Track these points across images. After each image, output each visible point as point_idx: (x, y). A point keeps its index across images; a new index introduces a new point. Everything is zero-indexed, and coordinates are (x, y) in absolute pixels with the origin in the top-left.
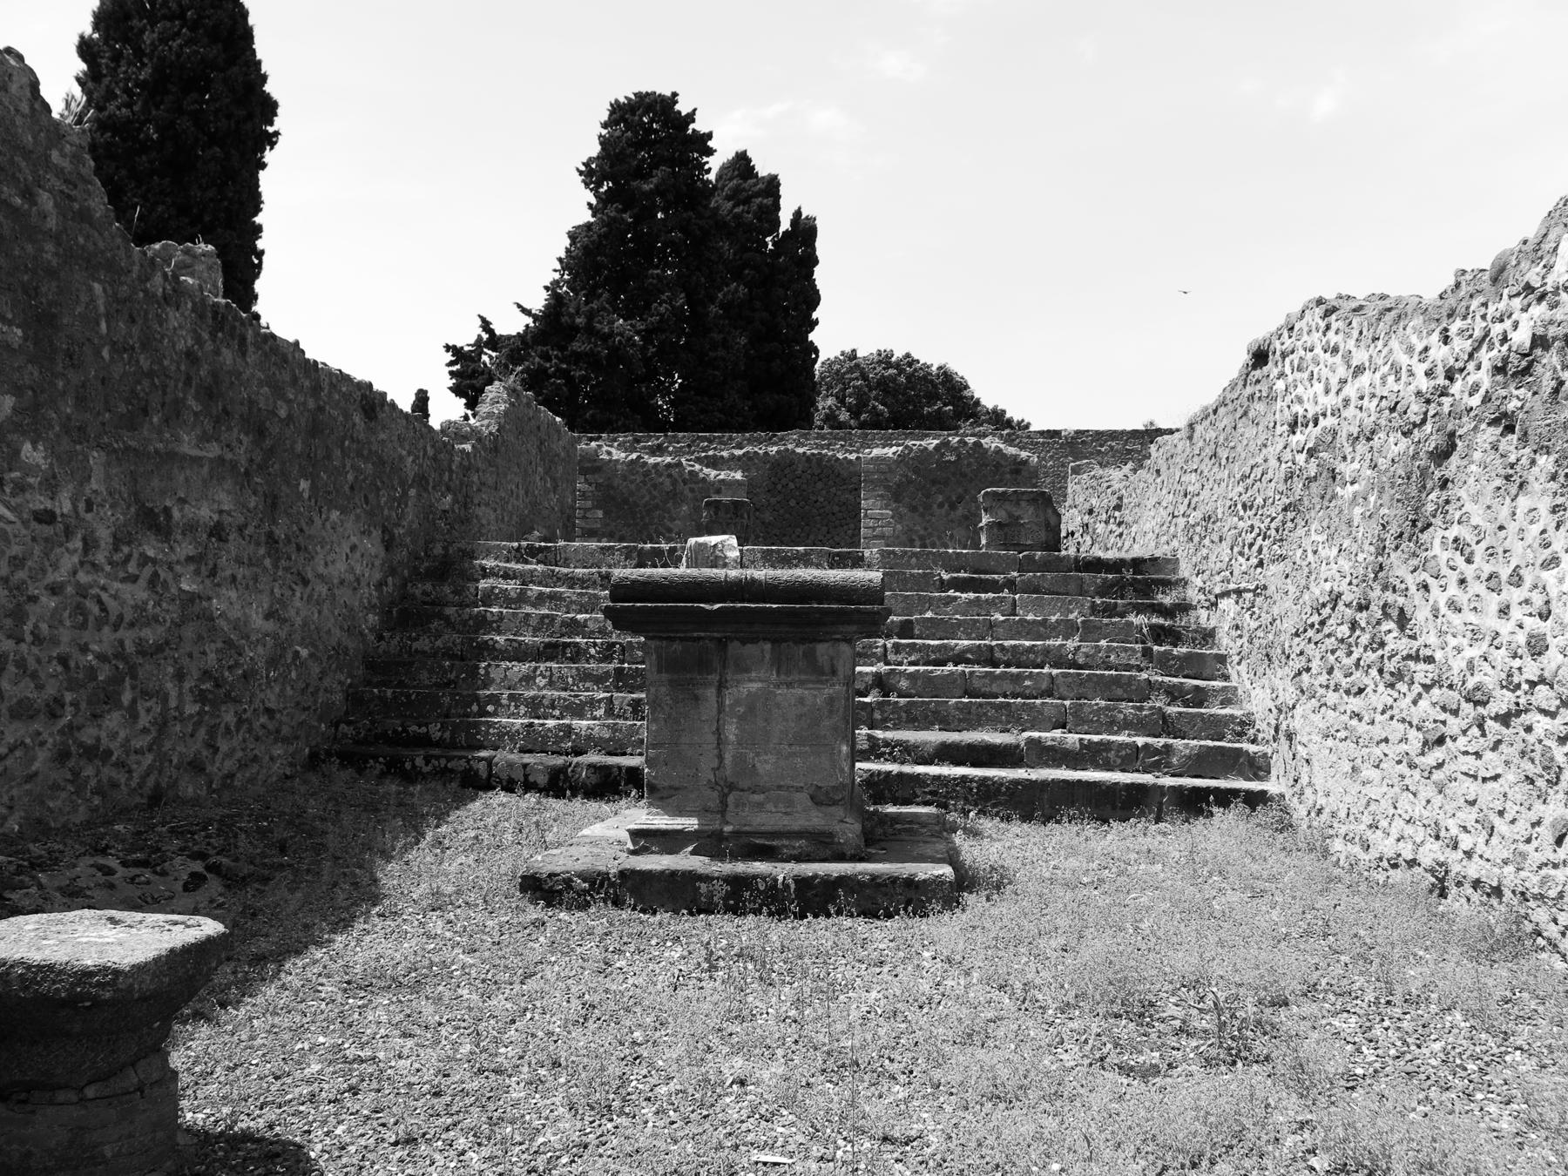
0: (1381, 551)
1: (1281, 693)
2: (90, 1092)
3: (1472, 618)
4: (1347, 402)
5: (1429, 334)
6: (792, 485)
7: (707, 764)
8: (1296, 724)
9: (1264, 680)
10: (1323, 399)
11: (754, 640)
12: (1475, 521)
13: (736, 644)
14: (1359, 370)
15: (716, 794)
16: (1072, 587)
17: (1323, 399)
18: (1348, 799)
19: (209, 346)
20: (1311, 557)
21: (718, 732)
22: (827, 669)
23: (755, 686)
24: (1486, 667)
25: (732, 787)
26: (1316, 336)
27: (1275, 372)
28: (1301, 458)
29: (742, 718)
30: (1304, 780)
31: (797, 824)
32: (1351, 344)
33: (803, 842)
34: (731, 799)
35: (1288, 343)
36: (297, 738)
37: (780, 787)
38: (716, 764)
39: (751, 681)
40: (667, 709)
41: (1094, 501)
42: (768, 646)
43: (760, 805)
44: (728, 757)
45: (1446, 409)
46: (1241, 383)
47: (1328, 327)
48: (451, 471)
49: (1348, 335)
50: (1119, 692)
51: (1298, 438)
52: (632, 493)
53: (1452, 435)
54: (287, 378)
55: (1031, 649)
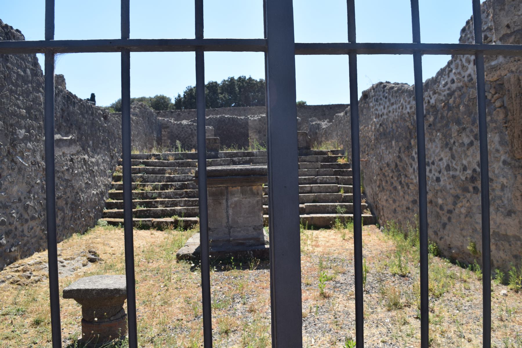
0: (400, 152)
2: (112, 318)
4: (390, 112)
5: (410, 97)
6: (224, 127)
7: (224, 221)
10: (383, 110)
11: (235, 187)
13: (231, 187)
14: (393, 104)
17: (383, 110)
21: (227, 212)
22: (256, 193)
25: (231, 227)
26: (381, 93)
29: (233, 208)
32: (390, 97)
34: (231, 230)
38: (227, 221)
39: (235, 197)
42: (239, 188)
43: (240, 232)
44: (230, 219)
49: (389, 94)
50: (330, 190)
52: (179, 134)
54: (85, 111)
55: (305, 179)
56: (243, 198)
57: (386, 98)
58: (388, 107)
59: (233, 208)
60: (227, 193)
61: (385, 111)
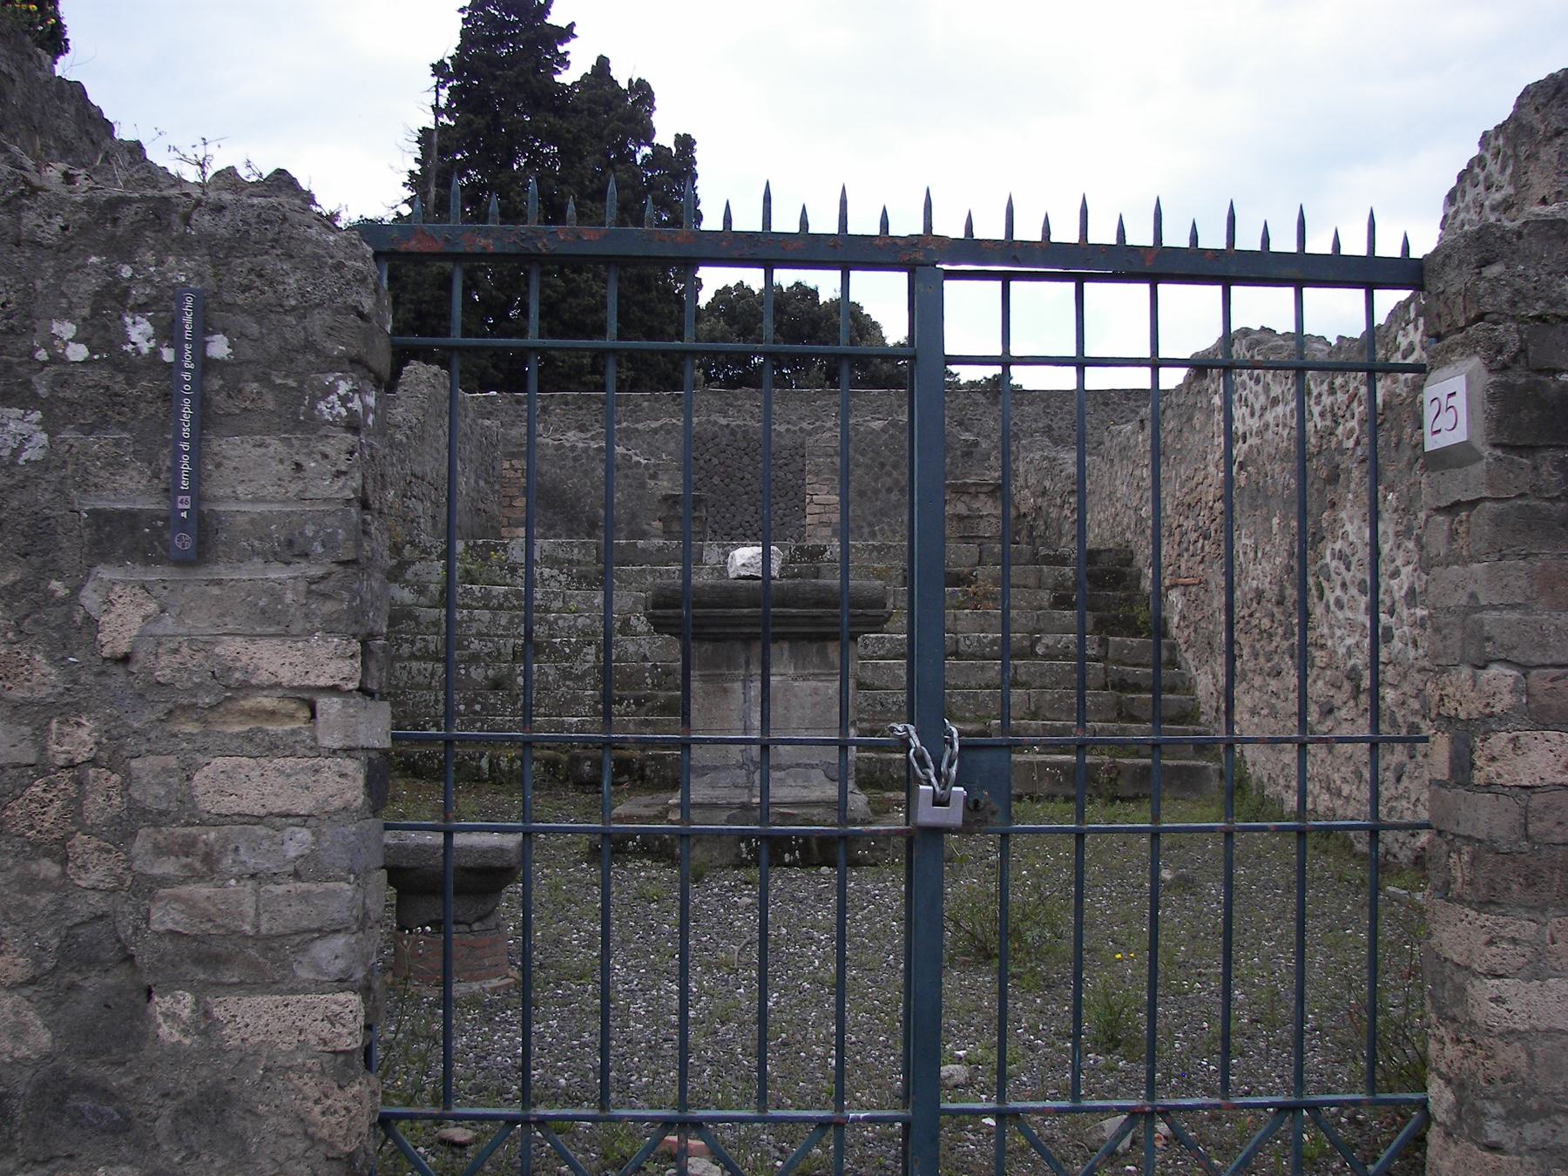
2: (476, 927)
3: (1350, 615)
12: (1352, 538)
14: (1275, 402)
16: (1032, 581)
17: (1249, 421)
18: (1269, 766)
24: (1358, 654)
27: (1213, 387)
31: (815, 795)
37: (798, 765)
41: (1047, 484)
42: (786, 645)
45: (1333, 445)
46: (1185, 391)
53: (1338, 466)
57: (1257, 381)
58: (1264, 409)
60: (748, 663)
61: (1255, 423)
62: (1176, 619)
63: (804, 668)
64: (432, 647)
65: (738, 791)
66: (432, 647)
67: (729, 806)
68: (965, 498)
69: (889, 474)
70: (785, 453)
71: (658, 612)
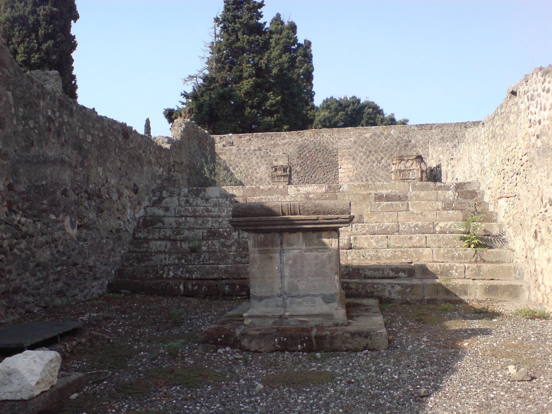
1: (528, 242)
6: (308, 155)
8: (536, 256)
9: (520, 237)
15: (281, 299)
19: (57, 114)
20: (539, 183)
21: (281, 271)
23: (296, 252)
27: (520, 100)
28: (533, 139)
30: (540, 281)
31: (317, 311)
33: (320, 318)
35: (526, 88)
36: (102, 277)
38: (280, 286)
39: (294, 249)
40: (258, 263)
42: (301, 234)
44: (286, 283)
47: (545, 80)
48: (161, 158)
51: (532, 129)
56: (306, 251)
59: (291, 266)
60: (281, 244)
62: (503, 213)
63: (310, 245)
64: (168, 235)
65: (279, 308)
66: (168, 235)
67: (273, 317)
68: (403, 162)
69: (373, 155)
70: (335, 151)
71: (235, 219)
